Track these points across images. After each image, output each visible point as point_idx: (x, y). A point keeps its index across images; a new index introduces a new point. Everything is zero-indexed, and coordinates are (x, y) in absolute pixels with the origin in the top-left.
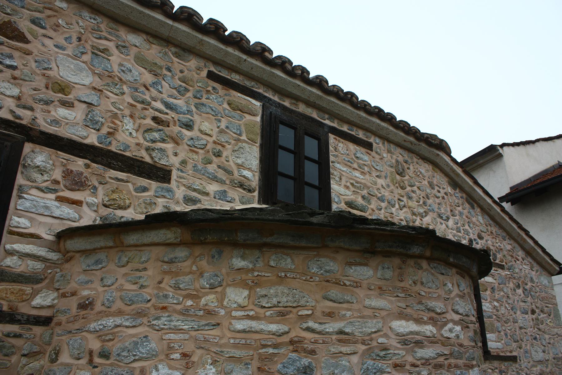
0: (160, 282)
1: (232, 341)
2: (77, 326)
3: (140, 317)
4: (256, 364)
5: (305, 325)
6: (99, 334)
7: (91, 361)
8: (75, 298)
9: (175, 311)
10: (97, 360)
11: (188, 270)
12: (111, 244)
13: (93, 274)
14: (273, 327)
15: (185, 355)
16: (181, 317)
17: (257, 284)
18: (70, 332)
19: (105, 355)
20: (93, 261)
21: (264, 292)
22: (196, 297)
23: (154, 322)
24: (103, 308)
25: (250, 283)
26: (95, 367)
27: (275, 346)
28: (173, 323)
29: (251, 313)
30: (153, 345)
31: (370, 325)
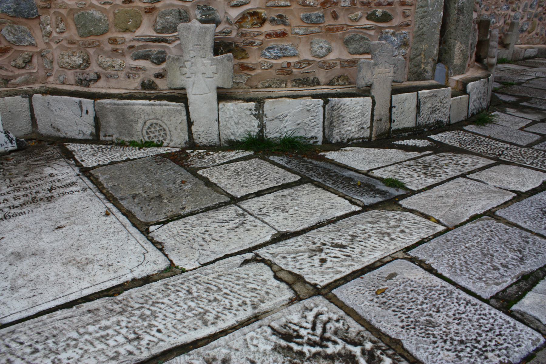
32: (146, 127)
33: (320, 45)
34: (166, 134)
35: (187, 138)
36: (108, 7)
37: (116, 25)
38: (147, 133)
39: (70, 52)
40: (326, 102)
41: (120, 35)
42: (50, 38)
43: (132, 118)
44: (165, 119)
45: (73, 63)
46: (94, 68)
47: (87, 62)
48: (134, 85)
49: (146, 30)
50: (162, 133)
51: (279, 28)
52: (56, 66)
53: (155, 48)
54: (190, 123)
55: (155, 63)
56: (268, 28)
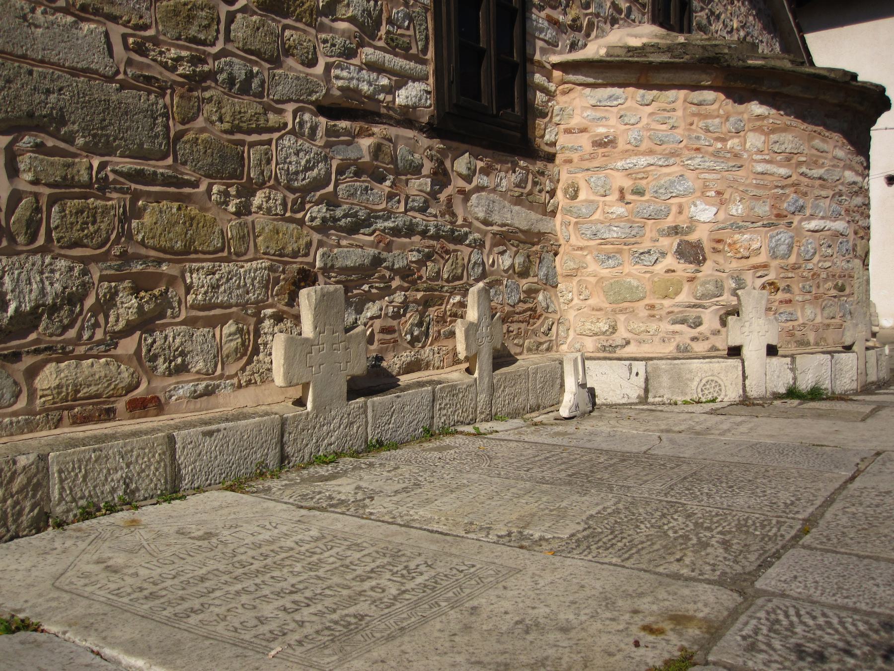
0: (691, 124)
1: (754, 182)
2: (596, 163)
3: (673, 156)
4: (769, 202)
5: (801, 171)
6: (629, 172)
7: (622, 198)
8: (585, 136)
9: (706, 152)
10: (629, 197)
11: (716, 113)
12: (633, 81)
13: (607, 110)
14: (783, 171)
15: (719, 193)
16: (713, 159)
17: (773, 131)
18: (588, 170)
19: (639, 192)
20: (606, 97)
21: (776, 139)
22: (723, 140)
23: (689, 162)
24: (629, 147)
25: (766, 130)
26: (627, 203)
27: (782, 188)
28: (707, 164)
29: (767, 157)
30: (690, 183)
31: (836, 173)
32: (702, 384)
33: (809, 311)
34: (720, 390)
35: (741, 392)
36: (648, 275)
37: (654, 293)
38: (702, 390)
39: (594, 320)
40: (832, 357)
41: (658, 301)
42: (571, 305)
43: (688, 376)
44: (722, 376)
45: (596, 330)
46: (622, 333)
47: (614, 329)
48: (669, 349)
49: (684, 297)
50: (717, 389)
51: (787, 296)
52: (571, 332)
53: (693, 313)
54: (744, 378)
55: (691, 327)
56: (780, 296)
